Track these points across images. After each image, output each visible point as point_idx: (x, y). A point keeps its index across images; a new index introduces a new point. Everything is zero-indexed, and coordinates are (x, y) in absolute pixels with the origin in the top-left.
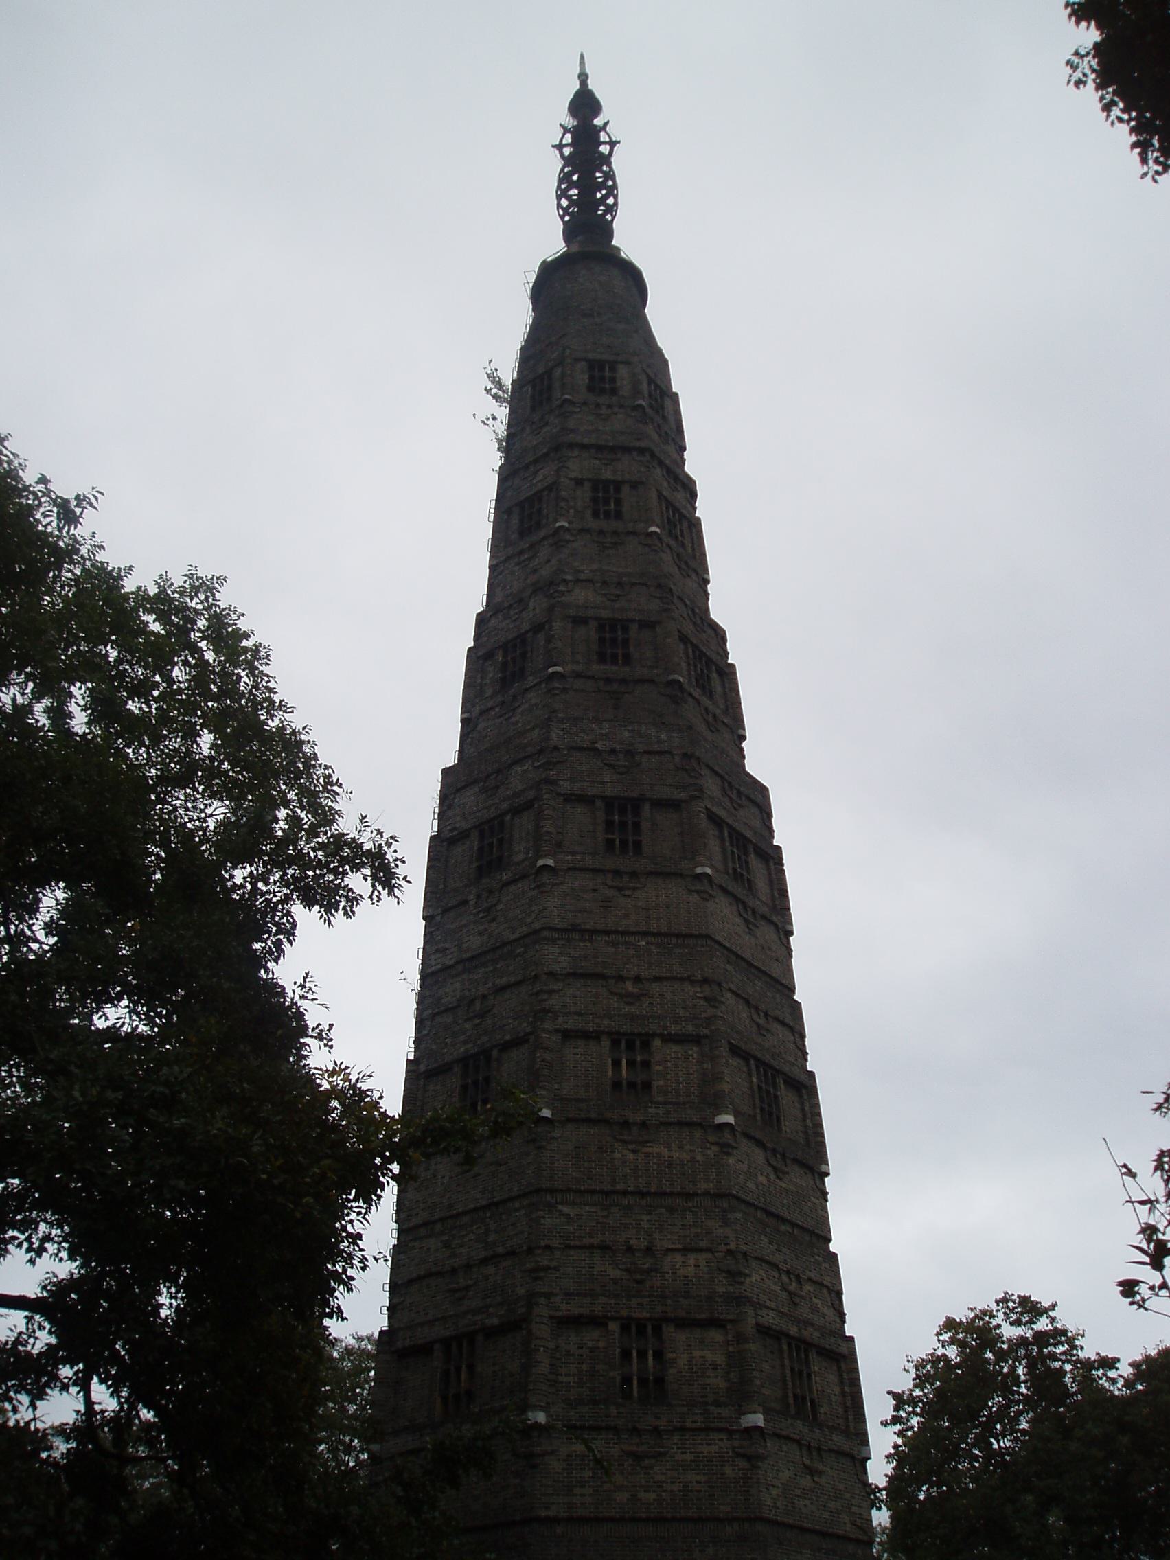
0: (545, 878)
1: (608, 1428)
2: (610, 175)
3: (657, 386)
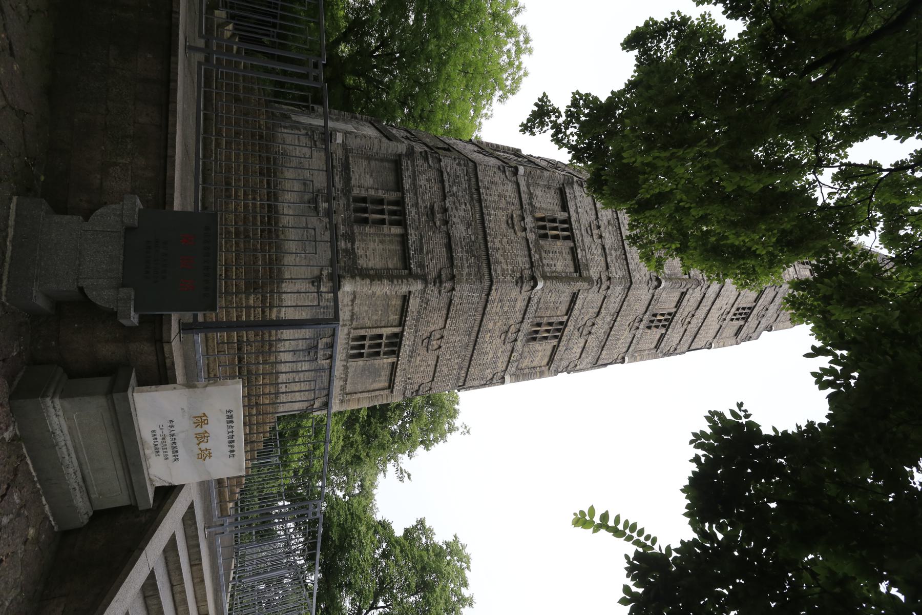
1: (523, 318)
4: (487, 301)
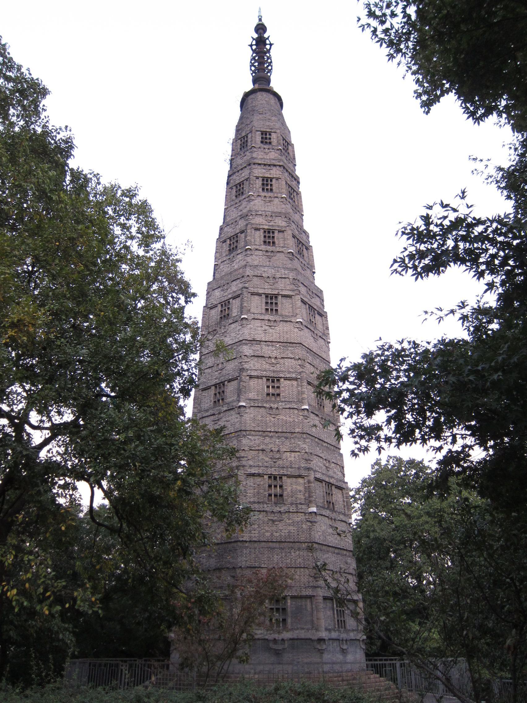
0: (244, 322)
1: (263, 511)
2: (269, 58)
3: (286, 141)
4: (250, 541)
